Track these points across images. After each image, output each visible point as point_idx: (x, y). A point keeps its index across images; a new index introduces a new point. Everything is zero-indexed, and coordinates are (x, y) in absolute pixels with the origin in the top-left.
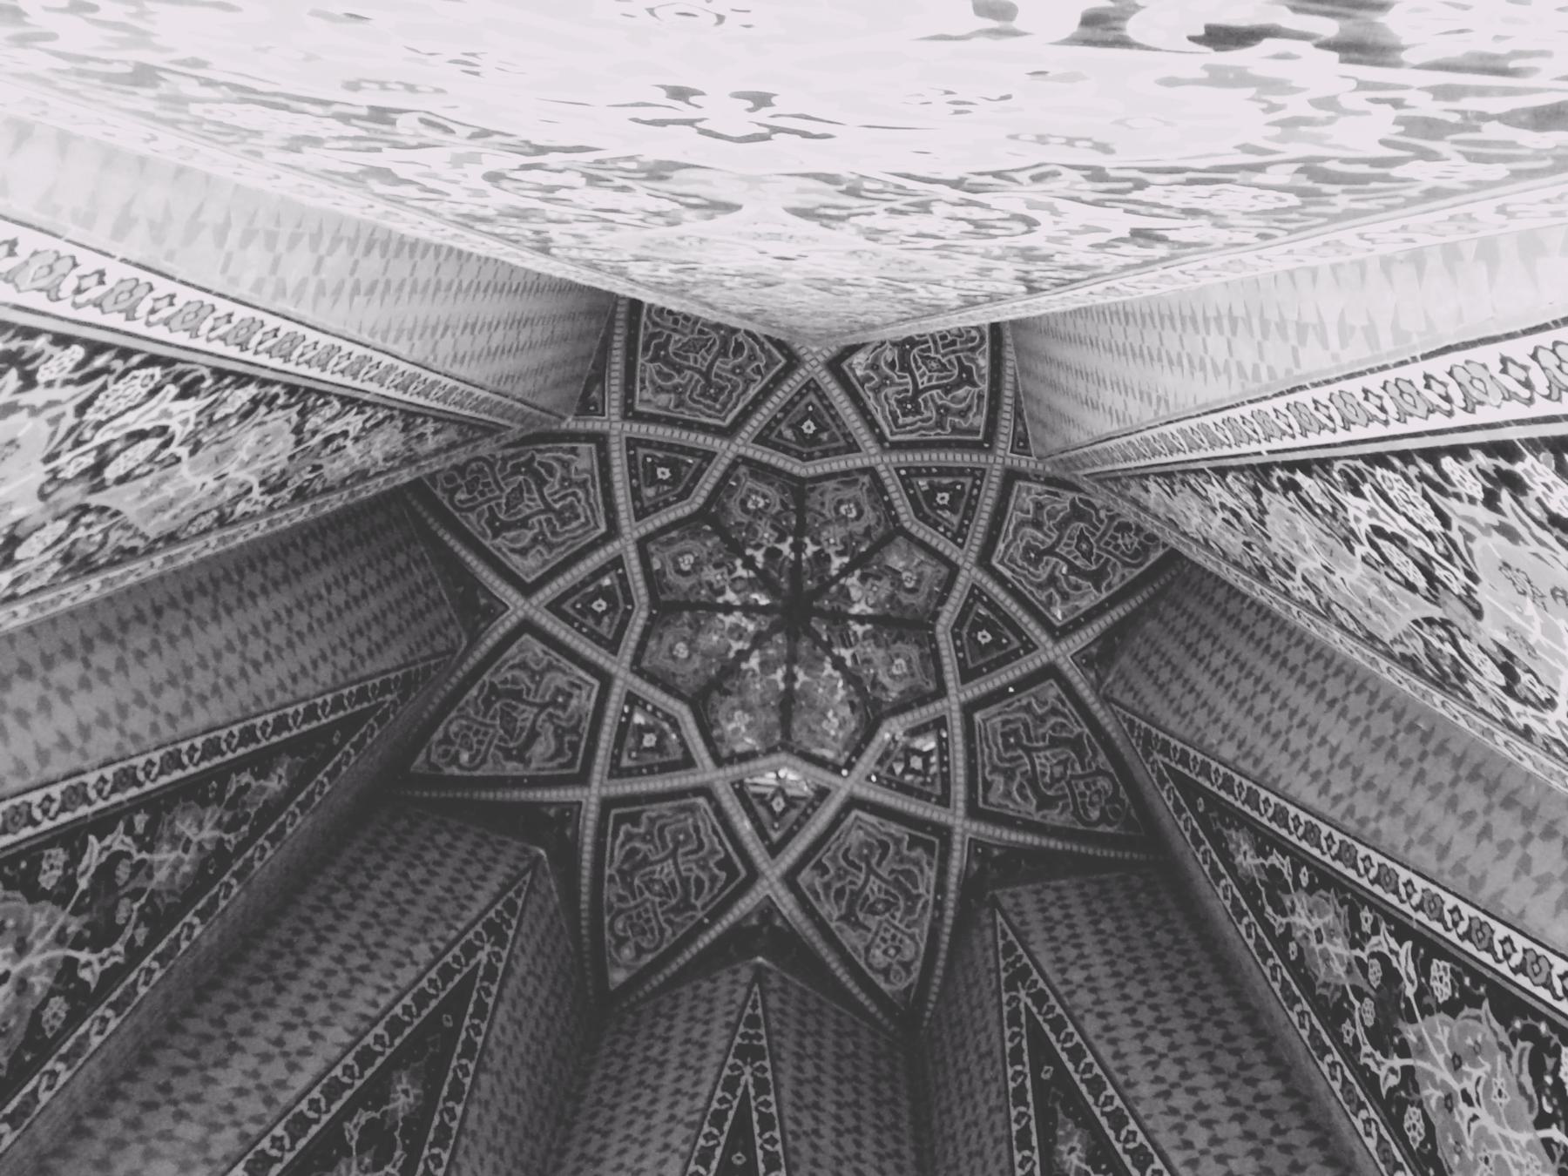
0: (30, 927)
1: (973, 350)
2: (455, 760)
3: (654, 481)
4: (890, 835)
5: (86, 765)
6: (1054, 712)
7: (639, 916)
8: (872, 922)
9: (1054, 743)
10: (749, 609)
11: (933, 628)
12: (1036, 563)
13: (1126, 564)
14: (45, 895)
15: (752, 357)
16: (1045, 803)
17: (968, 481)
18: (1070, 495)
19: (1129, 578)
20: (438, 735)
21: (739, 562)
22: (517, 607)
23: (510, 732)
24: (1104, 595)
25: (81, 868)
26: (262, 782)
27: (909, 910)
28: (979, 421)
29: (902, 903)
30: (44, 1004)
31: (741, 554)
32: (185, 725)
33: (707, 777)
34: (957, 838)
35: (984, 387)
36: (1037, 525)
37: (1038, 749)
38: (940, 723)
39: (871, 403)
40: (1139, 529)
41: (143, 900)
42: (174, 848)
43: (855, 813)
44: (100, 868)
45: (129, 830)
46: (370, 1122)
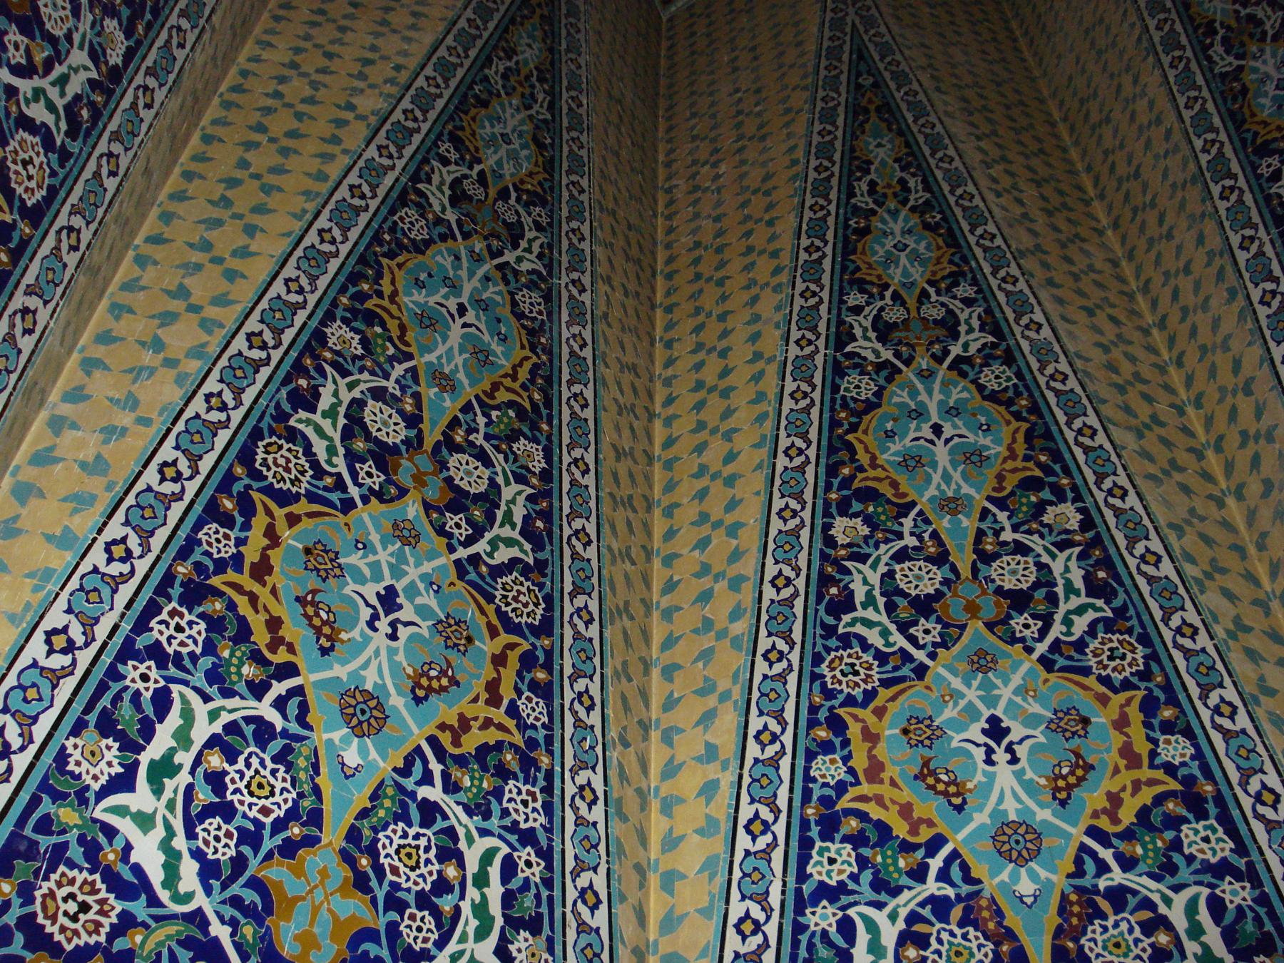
0: (902, 405)
5: (780, 358)
14: (879, 394)
25: (871, 357)
26: (873, 168)
30: (981, 388)
32: (786, 259)
41: (932, 291)
42: (896, 262)
44: (879, 339)
45: (857, 310)
46: (1225, 41)
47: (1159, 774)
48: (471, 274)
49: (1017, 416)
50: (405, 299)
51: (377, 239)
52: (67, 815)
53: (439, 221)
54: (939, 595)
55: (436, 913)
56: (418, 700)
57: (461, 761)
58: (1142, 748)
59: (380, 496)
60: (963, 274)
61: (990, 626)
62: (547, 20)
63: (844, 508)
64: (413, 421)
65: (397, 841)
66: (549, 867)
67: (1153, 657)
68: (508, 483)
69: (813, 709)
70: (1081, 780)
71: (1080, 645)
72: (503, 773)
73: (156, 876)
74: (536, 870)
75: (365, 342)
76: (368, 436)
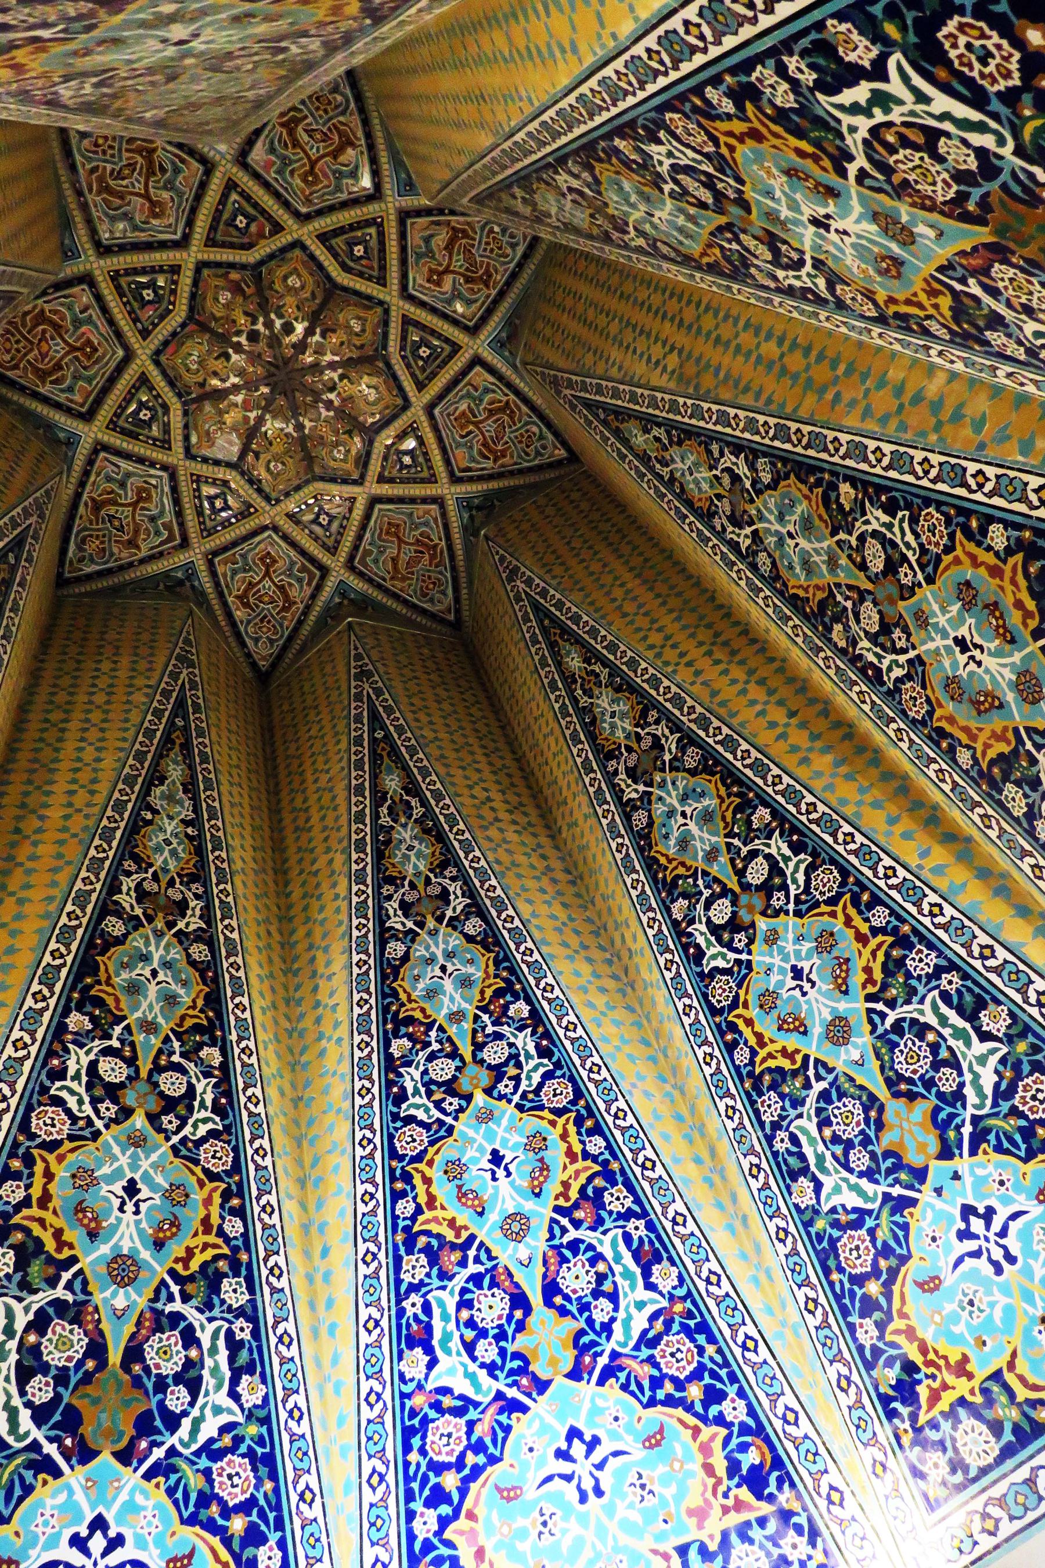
1: (249, 622)
2: (504, 231)
3: (411, 453)
4: (143, 230)
6: (70, 389)
7: (326, 111)
8: (125, 155)
9: (58, 367)
10: (316, 368)
11: (184, 404)
12: (140, 491)
13: (85, 529)
15: (376, 561)
16: (41, 318)
17: (209, 524)
18: (144, 553)
19: (77, 521)
20: (520, 250)
21: (336, 404)
22: (481, 345)
23: (467, 251)
24: (85, 497)
27: (101, 180)
28: (220, 570)
29: (111, 183)
31: (336, 410)
33: (305, 230)
34: (90, 252)
35: (230, 600)
36: (153, 519)
37: (67, 353)
38: (145, 334)
39: (292, 553)
40: (92, 561)
43: (178, 236)
47: (1011, 561)
48: (669, 794)
49: (787, 477)
50: (671, 852)
51: (642, 850)
52: (820, 1224)
53: (641, 799)
54: (880, 612)
55: (945, 1063)
56: (846, 993)
57: (885, 987)
58: (990, 559)
59: (751, 941)
60: (706, 444)
61: (903, 599)
62: (565, 631)
63: (830, 630)
64: (725, 892)
65: (902, 1059)
66: (958, 969)
67: (939, 505)
68: (768, 846)
69: (930, 737)
70: (1002, 617)
71: (924, 551)
72: (901, 962)
73: (860, 1203)
74: (955, 979)
75: (685, 895)
76: (722, 927)
